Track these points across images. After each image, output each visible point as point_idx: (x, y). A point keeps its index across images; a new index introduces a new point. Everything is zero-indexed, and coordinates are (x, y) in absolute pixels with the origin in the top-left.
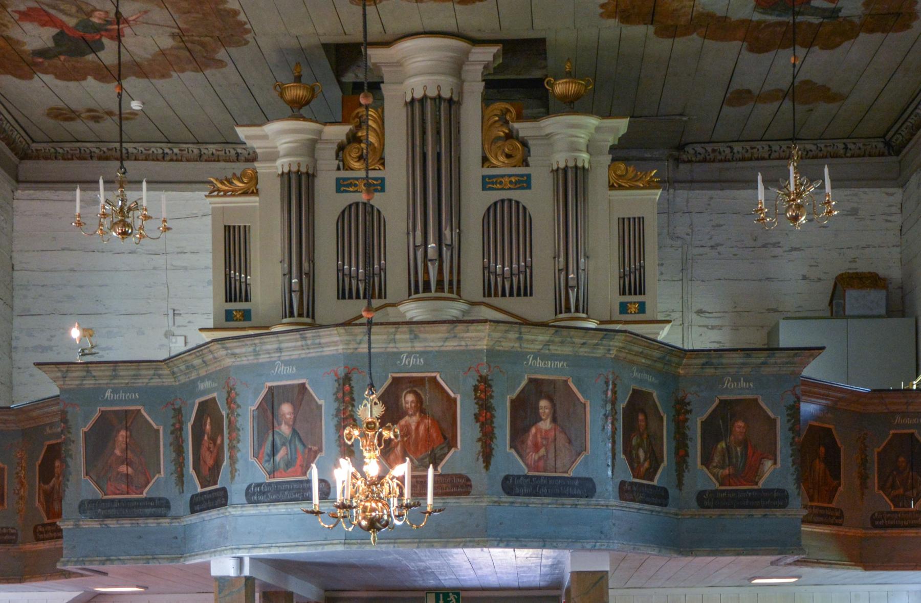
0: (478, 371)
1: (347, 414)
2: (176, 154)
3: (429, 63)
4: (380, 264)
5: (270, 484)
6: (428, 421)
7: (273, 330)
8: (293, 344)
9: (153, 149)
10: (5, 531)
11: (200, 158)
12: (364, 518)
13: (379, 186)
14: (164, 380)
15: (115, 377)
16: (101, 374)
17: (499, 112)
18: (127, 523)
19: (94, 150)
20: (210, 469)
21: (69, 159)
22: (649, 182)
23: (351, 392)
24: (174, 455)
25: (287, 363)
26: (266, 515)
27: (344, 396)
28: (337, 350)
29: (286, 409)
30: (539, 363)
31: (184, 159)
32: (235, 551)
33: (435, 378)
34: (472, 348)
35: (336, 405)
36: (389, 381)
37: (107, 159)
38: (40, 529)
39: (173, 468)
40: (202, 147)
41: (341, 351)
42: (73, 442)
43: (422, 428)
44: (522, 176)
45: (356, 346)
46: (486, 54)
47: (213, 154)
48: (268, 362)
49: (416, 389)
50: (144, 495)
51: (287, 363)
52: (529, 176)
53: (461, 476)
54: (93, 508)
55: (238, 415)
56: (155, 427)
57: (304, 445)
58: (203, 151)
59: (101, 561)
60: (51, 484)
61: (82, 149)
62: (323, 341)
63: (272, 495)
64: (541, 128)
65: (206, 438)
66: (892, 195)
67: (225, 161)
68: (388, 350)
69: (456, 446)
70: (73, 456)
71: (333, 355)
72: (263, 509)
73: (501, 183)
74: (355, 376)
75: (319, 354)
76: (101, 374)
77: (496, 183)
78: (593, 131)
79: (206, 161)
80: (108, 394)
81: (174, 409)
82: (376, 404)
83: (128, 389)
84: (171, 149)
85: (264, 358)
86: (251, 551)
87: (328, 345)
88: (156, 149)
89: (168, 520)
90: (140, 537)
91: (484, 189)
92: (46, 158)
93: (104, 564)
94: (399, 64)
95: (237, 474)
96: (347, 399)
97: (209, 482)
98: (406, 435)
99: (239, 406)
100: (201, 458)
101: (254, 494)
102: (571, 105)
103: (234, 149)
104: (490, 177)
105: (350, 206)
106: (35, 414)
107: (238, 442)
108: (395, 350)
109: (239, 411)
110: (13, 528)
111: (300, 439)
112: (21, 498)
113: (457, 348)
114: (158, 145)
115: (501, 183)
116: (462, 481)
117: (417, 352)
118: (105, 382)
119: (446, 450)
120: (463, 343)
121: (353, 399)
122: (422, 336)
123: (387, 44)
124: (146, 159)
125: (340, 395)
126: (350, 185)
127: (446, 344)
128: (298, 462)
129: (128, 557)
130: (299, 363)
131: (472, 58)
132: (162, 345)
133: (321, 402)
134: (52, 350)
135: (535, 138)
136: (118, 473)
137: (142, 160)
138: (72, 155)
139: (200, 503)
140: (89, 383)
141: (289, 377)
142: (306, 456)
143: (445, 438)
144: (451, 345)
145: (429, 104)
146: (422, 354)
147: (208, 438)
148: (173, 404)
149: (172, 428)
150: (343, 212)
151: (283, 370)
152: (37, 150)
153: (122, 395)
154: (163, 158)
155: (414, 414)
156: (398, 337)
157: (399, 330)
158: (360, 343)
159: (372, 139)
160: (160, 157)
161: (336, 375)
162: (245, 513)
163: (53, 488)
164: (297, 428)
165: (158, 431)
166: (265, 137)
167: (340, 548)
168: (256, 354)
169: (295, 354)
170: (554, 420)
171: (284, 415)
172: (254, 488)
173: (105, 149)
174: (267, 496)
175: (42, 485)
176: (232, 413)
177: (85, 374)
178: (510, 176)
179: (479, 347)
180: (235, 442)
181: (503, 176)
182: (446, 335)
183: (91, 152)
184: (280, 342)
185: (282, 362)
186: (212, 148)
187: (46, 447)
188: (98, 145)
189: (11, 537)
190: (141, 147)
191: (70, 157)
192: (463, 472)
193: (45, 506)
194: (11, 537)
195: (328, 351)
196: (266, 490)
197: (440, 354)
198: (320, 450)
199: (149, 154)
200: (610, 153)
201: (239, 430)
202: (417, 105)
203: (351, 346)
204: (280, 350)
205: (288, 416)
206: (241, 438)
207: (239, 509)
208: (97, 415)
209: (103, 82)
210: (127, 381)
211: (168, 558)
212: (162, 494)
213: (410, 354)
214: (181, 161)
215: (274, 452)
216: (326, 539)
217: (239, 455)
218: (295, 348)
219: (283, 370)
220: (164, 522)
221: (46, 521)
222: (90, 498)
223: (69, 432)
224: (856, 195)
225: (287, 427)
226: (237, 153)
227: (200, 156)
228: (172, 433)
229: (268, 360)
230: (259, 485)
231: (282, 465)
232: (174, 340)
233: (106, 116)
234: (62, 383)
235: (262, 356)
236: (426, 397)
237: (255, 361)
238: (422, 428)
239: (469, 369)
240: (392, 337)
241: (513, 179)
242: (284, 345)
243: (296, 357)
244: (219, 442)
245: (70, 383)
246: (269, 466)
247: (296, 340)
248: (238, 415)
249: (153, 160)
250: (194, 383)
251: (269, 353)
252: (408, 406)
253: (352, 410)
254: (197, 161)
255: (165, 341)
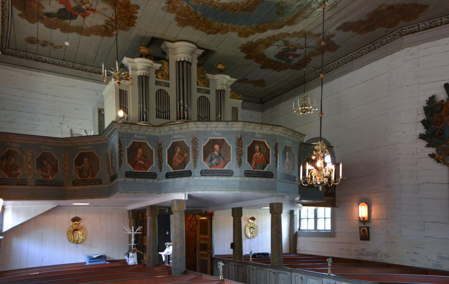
0: (276, 141)
1: (240, 150)
2: (64, 65)
3: (186, 51)
4: (167, 109)
5: (210, 170)
6: (262, 155)
7: (176, 123)
8: (222, 126)
9: (56, 61)
10: (58, 182)
11: (73, 67)
12: (320, 182)
13: (168, 85)
14: (155, 133)
15: (139, 130)
16: (134, 128)
17: (201, 70)
18: (143, 180)
19: (32, 56)
20: (179, 164)
21: (21, 58)
22: (240, 98)
23: (242, 143)
24: (158, 159)
25: (217, 132)
26: (208, 180)
27: (239, 144)
28: (238, 129)
29: (217, 147)
30: (287, 141)
31: (67, 67)
32: (197, 191)
33: (264, 142)
34: (274, 134)
35: (237, 147)
36: (252, 141)
37: (37, 61)
38: (76, 181)
39: (158, 163)
40: (74, 64)
41: (239, 130)
42: (123, 151)
43: (260, 157)
44: (208, 90)
45: (244, 129)
46: (200, 52)
47: (77, 67)
48: (210, 131)
49: (259, 145)
50: (148, 171)
51: (217, 132)
52: (209, 90)
53: (271, 172)
54: (128, 175)
55: (198, 147)
56: (152, 149)
57: (223, 158)
58: (74, 65)
59: (134, 193)
60: (82, 166)
61: (27, 55)
62: (234, 126)
63: (211, 174)
64: (214, 77)
65: (177, 154)
66: (259, 114)
67: (82, 70)
68: (253, 131)
69: (269, 163)
70: (123, 156)
71: (235, 131)
72: (208, 178)
73: (202, 91)
74: (243, 138)
75: (230, 130)
76: (134, 128)
77: (201, 91)
78: (227, 80)
79: (75, 69)
80: (135, 136)
81: (158, 144)
82: (323, 145)
83: (143, 135)
84: (62, 62)
85: (209, 129)
86: (204, 191)
87: (235, 127)
88: (57, 61)
89: (157, 180)
90: (147, 185)
91: (198, 92)
92: (11, 55)
93: (150, 194)
94: (174, 49)
95: (197, 166)
96: (240, 145)
97: (179, 168)
98: (256, 159)
99: (198, 144)
100: (173, 160)
101: (204, 173)
102: (221, 72)
103: (85, 67)
104: (200, 89)
105: (159, 90)
106: (74, 141)
107: (198, 156)
108: (254, 132)
109: (198, 146)
110: (62, 181)
111: (222, 157)
112: (65, 170)
113: (271, 134)
114: (58, 60)
115: (202, 91)
116: (271, 174)
117: (260, 133)
118: (135, 131)
119: (267, 164)
120: (273, 132)
121: (242, 145)
122: (263, 128)
123: (173, 42)
124: (53, 64)
125: (238, 144)
126: (160, 83)
127: (268, 132)
128: (221, 164)
129: (143, 192)
130: (223, 133)
131: (196, 52)
132: (59, 127)
133: (231, 146)
134: (15, 123)
135: (212, 80)
136: (139, 163)
137: (51, 64)
138: (23, 57)
139: (169, 175)
140: (129, 131)
141: (218, 136)
142: (224, 162)
143: (267, 161)
144: (270, 133)
145: (185, 64)
146: (261, 134)
147: (178, 153)
148: (158, 142)
149: (158, 150)
150: (157, 92)
151: (216, 134)
152: (8, 52)
153: (141, 137)
154: (59, 65)
155: (258, 152)
156: (257, 128)
157: (259, 125)
158: (245, 128)
159: (166, 71)
160: (58, 64)
161: (237, 137)
162: (200, 179)
163: (83, 167)
164: (221, 152)
165: (152, 150)
166: (134, 63)
167: (238, 192)
168: (207, 127)
169: (221, 129)
170: (289, 158)
171: (216, 148)
172: (204, 171)
173: (37, 57)
174: (209, 174)
175: (77, 166)
176: (195, 146)
177: (129, 128)
178: (204, 89)
179: (276, 134)
180: (196, 156)
181: (203, 89)
182: (270, 129)
183: (31, 57)
184: (218, 124)
185: (216, 131)
186: (78, 65)
187: (79, 154)
188: (35, 55)
189: (61, 184)
190: (51, 60)
191: (22, 57)
192: (272, 171)
193: (79, 174)
194: (61, 184)
195: (234, 129)
196: (209, 172)
197: (266, 135)
198: (230, 160)
199: (54, 63)
200: (230, 88)
201: (198, 152)
202: (181, 64)
203: (243, 129)
204: (216, 127)
205: (217, 149)
206: (199, 155)
207: (199, 178)
208: (132, 142)
209: (64, 32)
210: (142, 132)
211: (157, 193)
212: (154, 172)
213: (258, 134)
214: (66, 67)
215: (212, 159)
216: (232, 189)
217: (198, 160)
218: (222, 127)
219: (216, 134)
220: (155, 181)
221: (79, 179)
222: (129, 171)
223: (122, 148)
224: (252, 112)
225: (217, 152)
226: (86, 69)
227: (73, 67)
228: (157, 151)
229: (211, 130)
230: (206, 170)
231: (215, 164)
232: (64, 125)
233: (49, 45)
234: (119, 130)
235: (208, 129)
236: (262, 147)
237: (205, 130)
238: (260, 157)
239: (274, 140)
240: (255, 127)
241: (205, 91)
242: (218, 126)
243: (222, 130)
244: (185, 155)
245: (122, 130)
246: (210, 164)
247: (224, 125)
248: (198, 147)
249: (55, 65)
250: (171, 135)
251: (211, 128)
252: (257, 149)
253: (242, 149)
254: (71, 68)
255: (60, 125)
